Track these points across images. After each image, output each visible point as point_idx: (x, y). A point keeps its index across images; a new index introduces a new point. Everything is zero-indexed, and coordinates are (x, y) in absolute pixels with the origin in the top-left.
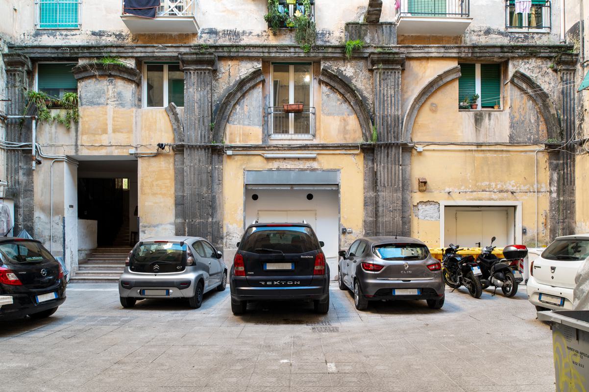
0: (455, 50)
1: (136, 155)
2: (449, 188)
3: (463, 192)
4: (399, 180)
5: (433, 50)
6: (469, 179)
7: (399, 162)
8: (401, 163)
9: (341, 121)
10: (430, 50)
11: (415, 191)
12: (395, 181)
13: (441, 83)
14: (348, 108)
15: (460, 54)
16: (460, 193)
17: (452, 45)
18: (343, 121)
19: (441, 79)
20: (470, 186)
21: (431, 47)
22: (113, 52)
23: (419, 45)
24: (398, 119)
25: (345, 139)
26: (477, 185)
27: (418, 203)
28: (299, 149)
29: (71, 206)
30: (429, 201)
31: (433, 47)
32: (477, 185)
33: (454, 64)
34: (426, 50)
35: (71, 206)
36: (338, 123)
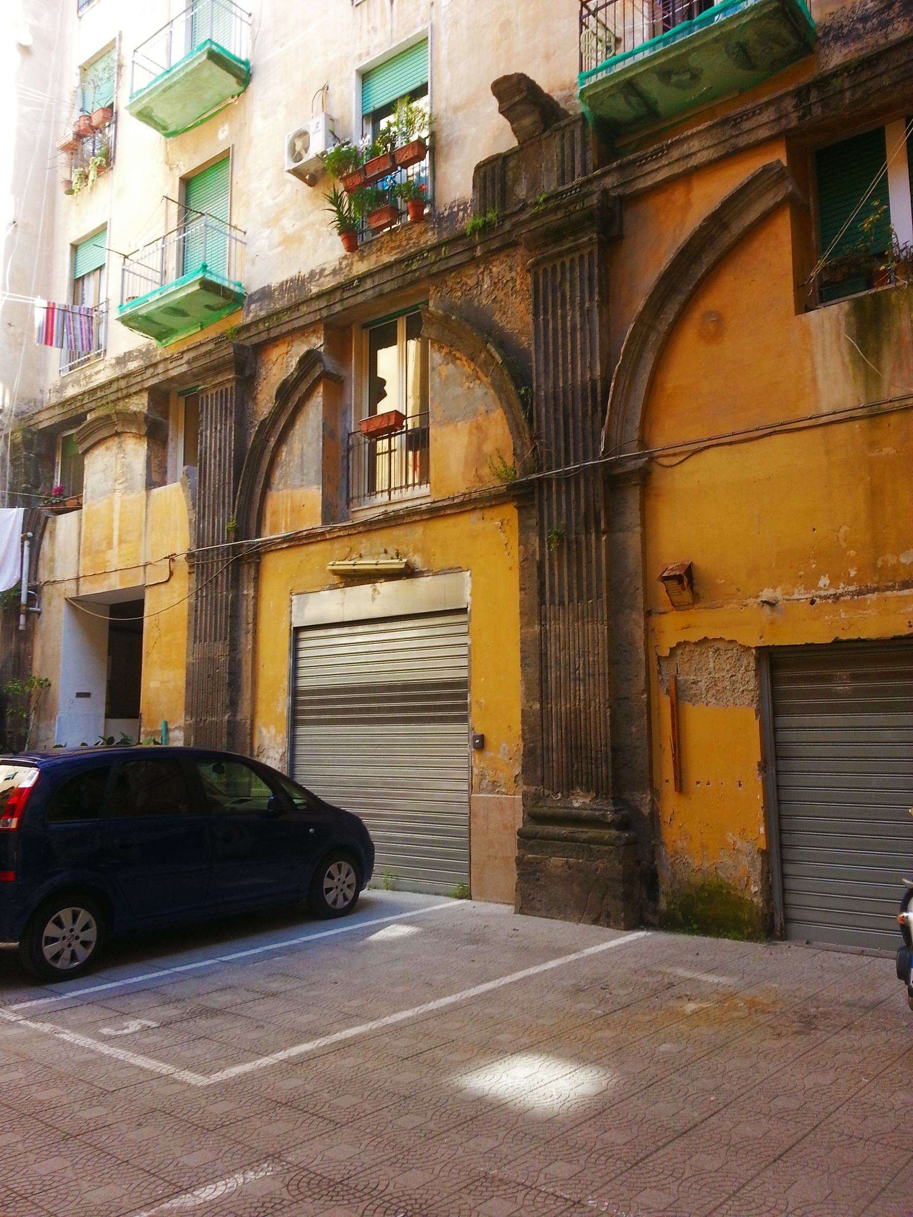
0: (768, 116)
1: (144, 587)
2: (774, 588)
3: (826, 597)
4: (599, 580)
5: (695, 145)
6: (844, 545)
7: (598, 524)
8: (603, 526)
9: (470, 433)
10: (685, 149)
11: (662, 609)
12: (589, 584)
13: (727, 239)
14: (486, 394)
15: (784, 122)
16: (813, 602)
17: (749, 106)
18: (475, 432)
19: (725, 227)
20: (853, 573)
21: (687, 139)
22: (694, 154)
23: (651, 149)
24: (594, 390)
25: (479, 478)
26: (880, 563)
27: (673, 650)
28: (384, 525)
29: (667, 781)
30: (705, 639)
31: (693, 135)
32: (880, 563)
33: (779, 156)
34: (675, 154)
35: (667, 781)
36: (465, 439)
